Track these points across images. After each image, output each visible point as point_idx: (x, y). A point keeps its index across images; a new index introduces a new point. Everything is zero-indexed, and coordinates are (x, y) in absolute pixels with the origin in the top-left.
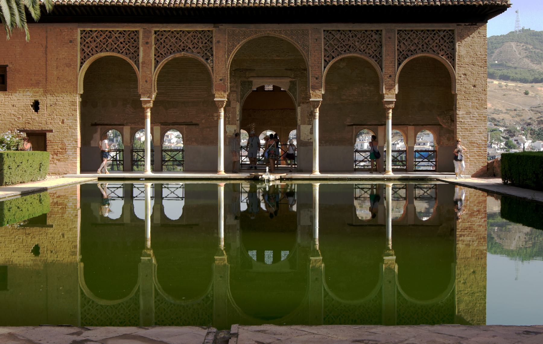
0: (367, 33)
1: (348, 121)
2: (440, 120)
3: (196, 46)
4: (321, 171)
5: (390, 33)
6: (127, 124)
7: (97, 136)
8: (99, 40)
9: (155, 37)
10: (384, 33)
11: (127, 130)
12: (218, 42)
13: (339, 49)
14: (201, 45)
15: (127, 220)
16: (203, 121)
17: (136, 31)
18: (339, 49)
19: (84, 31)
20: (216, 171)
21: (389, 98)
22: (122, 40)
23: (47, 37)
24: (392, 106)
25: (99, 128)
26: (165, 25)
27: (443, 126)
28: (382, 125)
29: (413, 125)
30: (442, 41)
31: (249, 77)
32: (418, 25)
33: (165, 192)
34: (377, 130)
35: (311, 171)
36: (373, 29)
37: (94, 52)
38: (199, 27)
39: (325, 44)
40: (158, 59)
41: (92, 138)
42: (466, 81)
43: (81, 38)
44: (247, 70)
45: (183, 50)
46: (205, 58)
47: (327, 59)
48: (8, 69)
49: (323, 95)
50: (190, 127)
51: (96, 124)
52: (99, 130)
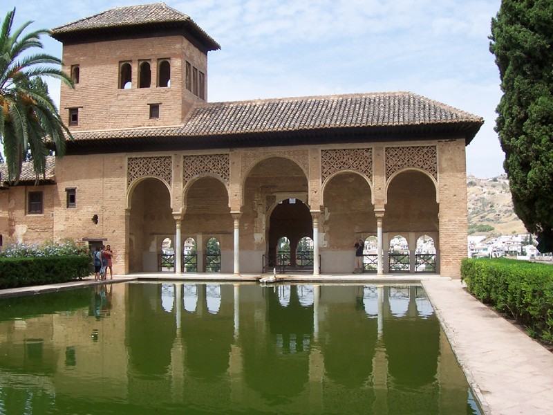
4: (320, 273)
5: (378, 152)
7: (154, 243)
9: (184, 161)
10: (373, 151)
12: (234, 163)
13: (335, 166)
14: (220, 166)
17: (170, 157)
18: (335, 166)
20: (232, 272)
21: (381, 208)
22: (158, 164)
23: (104, 165)
25: (156, 236)
28: (387, 232)
31: (272, 193)
32: (403, 142)
33: (208, 289)
35: (312, 273)
36: (364, 147)
37: (138, 175)
41: (150, 245)
42: (447, 192)
43: (129, 164)
46: (224, 177)
47: (325, 175)
48: (76, 190)
49: (321, 206)
50: (226, 235)
51: (153, 234)
52: (156, 239)
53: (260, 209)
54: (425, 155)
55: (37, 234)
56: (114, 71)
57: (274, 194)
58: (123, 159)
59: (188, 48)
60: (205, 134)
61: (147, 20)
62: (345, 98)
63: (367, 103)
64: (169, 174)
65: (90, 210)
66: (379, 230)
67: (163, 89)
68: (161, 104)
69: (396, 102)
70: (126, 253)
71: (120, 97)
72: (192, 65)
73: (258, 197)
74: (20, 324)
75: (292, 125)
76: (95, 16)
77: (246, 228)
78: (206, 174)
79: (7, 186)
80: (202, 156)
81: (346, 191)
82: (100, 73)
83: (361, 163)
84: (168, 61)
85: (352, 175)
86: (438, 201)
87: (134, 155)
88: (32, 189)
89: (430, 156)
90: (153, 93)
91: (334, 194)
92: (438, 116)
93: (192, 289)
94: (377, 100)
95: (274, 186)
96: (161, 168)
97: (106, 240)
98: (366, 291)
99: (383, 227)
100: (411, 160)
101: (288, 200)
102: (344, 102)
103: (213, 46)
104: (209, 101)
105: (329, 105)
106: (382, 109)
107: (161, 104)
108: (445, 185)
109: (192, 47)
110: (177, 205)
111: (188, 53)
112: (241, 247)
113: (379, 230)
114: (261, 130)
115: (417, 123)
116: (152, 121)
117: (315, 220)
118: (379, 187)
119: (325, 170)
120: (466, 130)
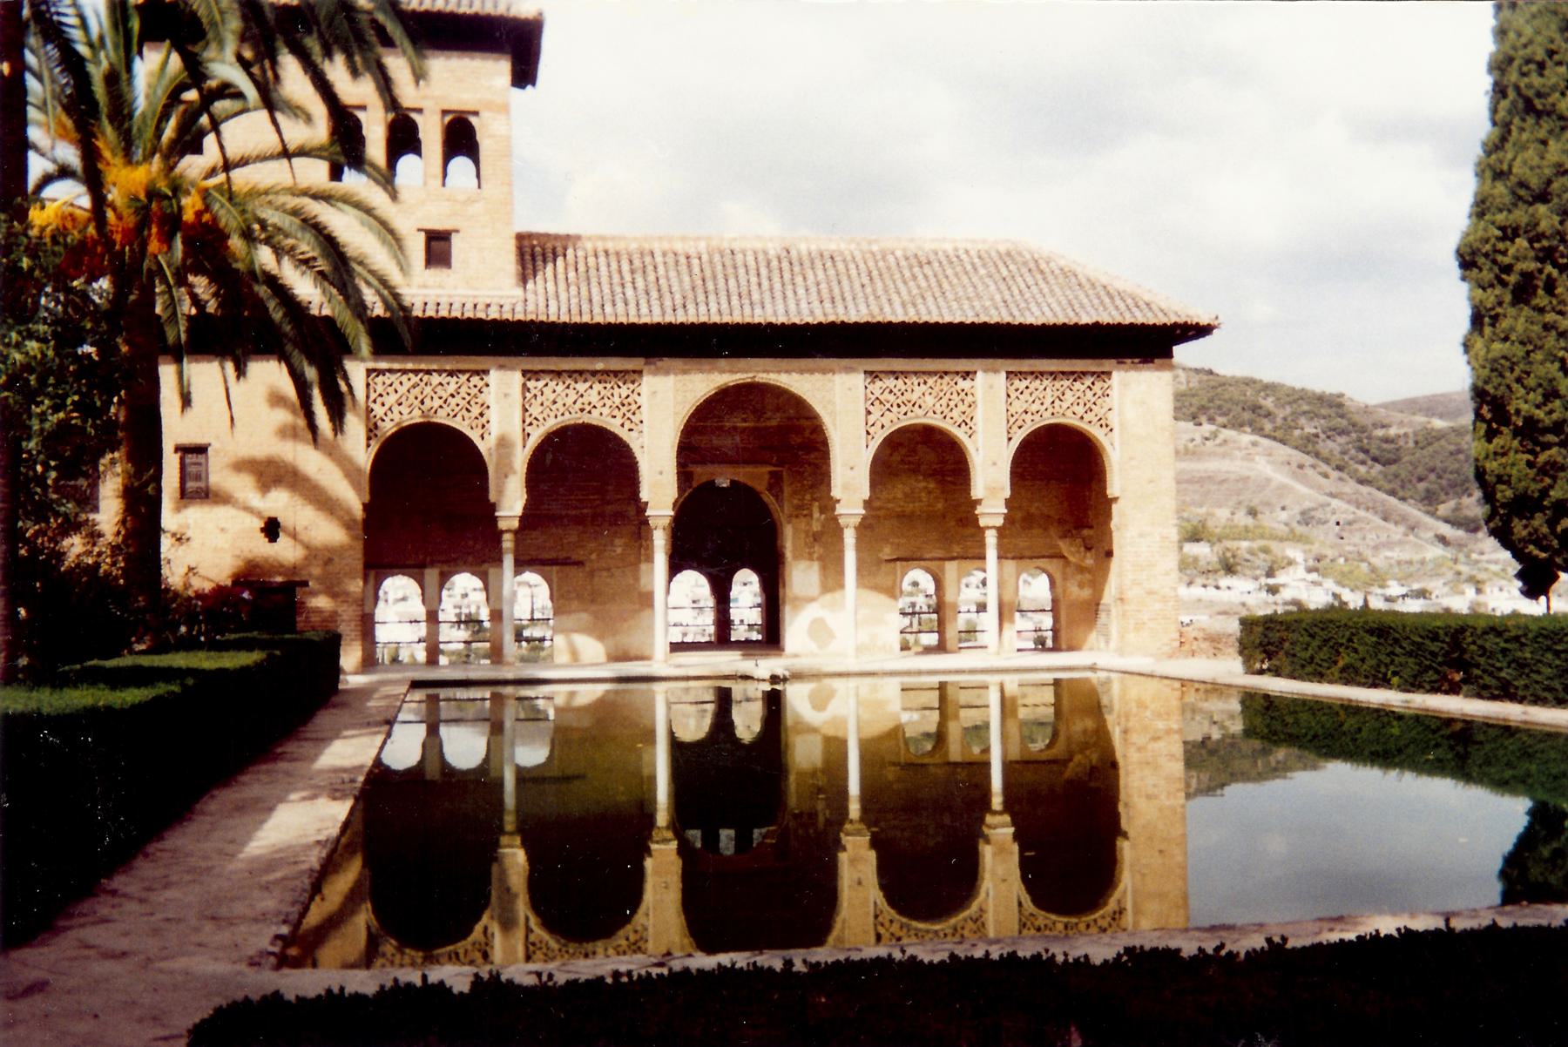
0: (947, 378)
1: (887, 552)
2: (1064, 546)
3: (609, 403)
6: (432, 564)
8: (402, 390)
11: (431, 574)
14: (617, 401)
15: (432, 772)
16: (594, 556)
18: (895, 409)
19: (374, 370)
22: (452, 388)
24: (999, 522)
26: (544, 359)
27: (1071, 559)
29: (1013, 558)
34: (943, 570)
38: (616, 363)
39: (866, 399)
40: (528, 429)
45: (582, 410)
47: (872, 430)
49: (865, 502)
50: (567, 569)
64: (482, 415)
66: (991, 553)
68: (457, 231)
77: (619, 550)
78: (585, 419)
80: (571, 373)
81: (923, 463)
83: (952, 404)
84: (473, 120)
89: (1099, 393)
96: (458, 399)
99: (1000, 546)
107: (457, 231)
108: (1132, 458)
113: (991, 553)
119: (872, 419)
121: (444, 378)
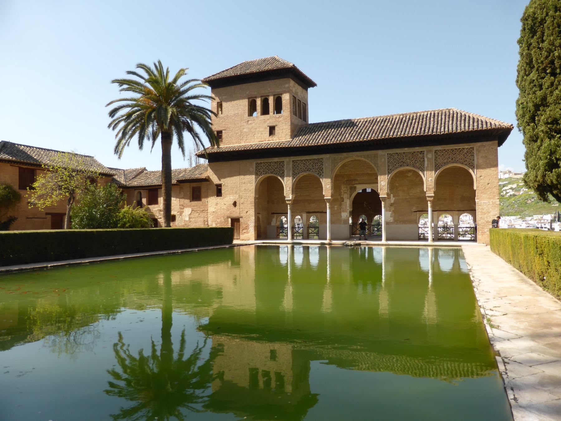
0: (414, 154)
1: (414, 209)
4: (387, 240)
7: (274, 220)
14: (317, 167)
22: (276, 167)
24: (432, 199)
25: (275, 215)
30: (466, 155)
32: (449, 146)
35: (381, 240)
39: (388, 162)
41: (272, 221)
44: (353, 180)
53: (345, 196)
54: (466, 155)
55: (198, 214)
56: (244, 104)
57: (355, 185)
58: (252, 164)
59: (294, 86)
60: (306, 145)
61: (266, 68)
62: (404, 115)
63: (421, 118)
65: (232, 198)
66: (430, 210)
67: (278, 115)
69: (443, 117)
70: (255, 226)
71: (249, 122)
72: (297, 98)
73: (343, 188)
74: (188, 273)
75: (366, 137)
76: (231, 68)
79: (178, 183)
82: (236, 108)
85: (410, 171)
86: (475, 188)
87: (259, 161)
88: (195, 185)
90: (271, 118)
91: (397, 185)
92: (476, 124)
93: (299, 250)
94: (429, 116)
95: (355, 180)
97: (242, 217)
98: (421, 252)
99: (432, 207)
100: (454, 159)
101: (366, 189)
102: (404, 119)
103: (313, 84)
104: (309, 123)
105: (393, 122)
106: (432, 123)
109: (297, 86)
110: (289, 195)
111: (294, 90)
112: (332, 222)
113: (430, 210)
114: (344, 141)
115: (459, 131)
116: (271, 138)
117: (383, 203)
118: (429, 178)
119: (390, 167)
120: (500, 135)
121: (274, 164)
